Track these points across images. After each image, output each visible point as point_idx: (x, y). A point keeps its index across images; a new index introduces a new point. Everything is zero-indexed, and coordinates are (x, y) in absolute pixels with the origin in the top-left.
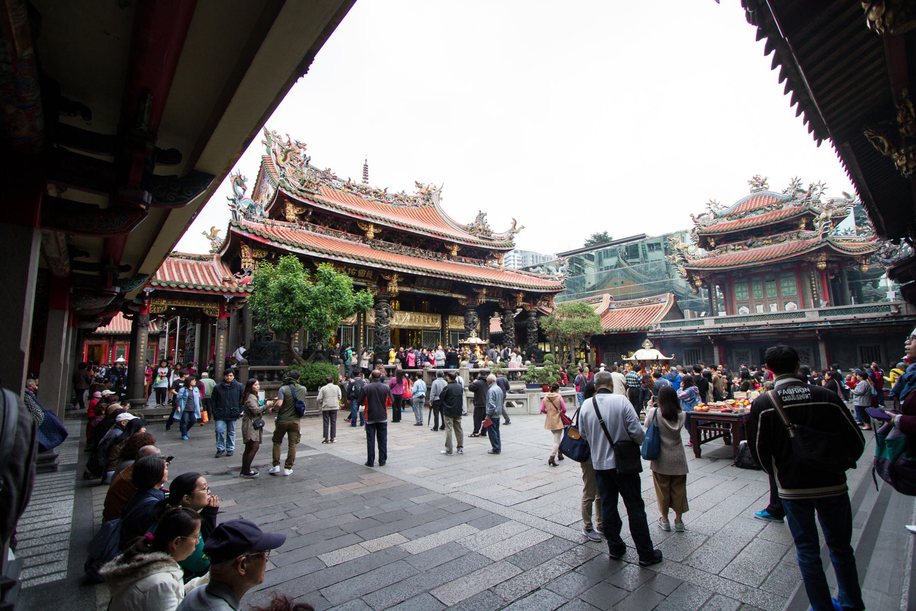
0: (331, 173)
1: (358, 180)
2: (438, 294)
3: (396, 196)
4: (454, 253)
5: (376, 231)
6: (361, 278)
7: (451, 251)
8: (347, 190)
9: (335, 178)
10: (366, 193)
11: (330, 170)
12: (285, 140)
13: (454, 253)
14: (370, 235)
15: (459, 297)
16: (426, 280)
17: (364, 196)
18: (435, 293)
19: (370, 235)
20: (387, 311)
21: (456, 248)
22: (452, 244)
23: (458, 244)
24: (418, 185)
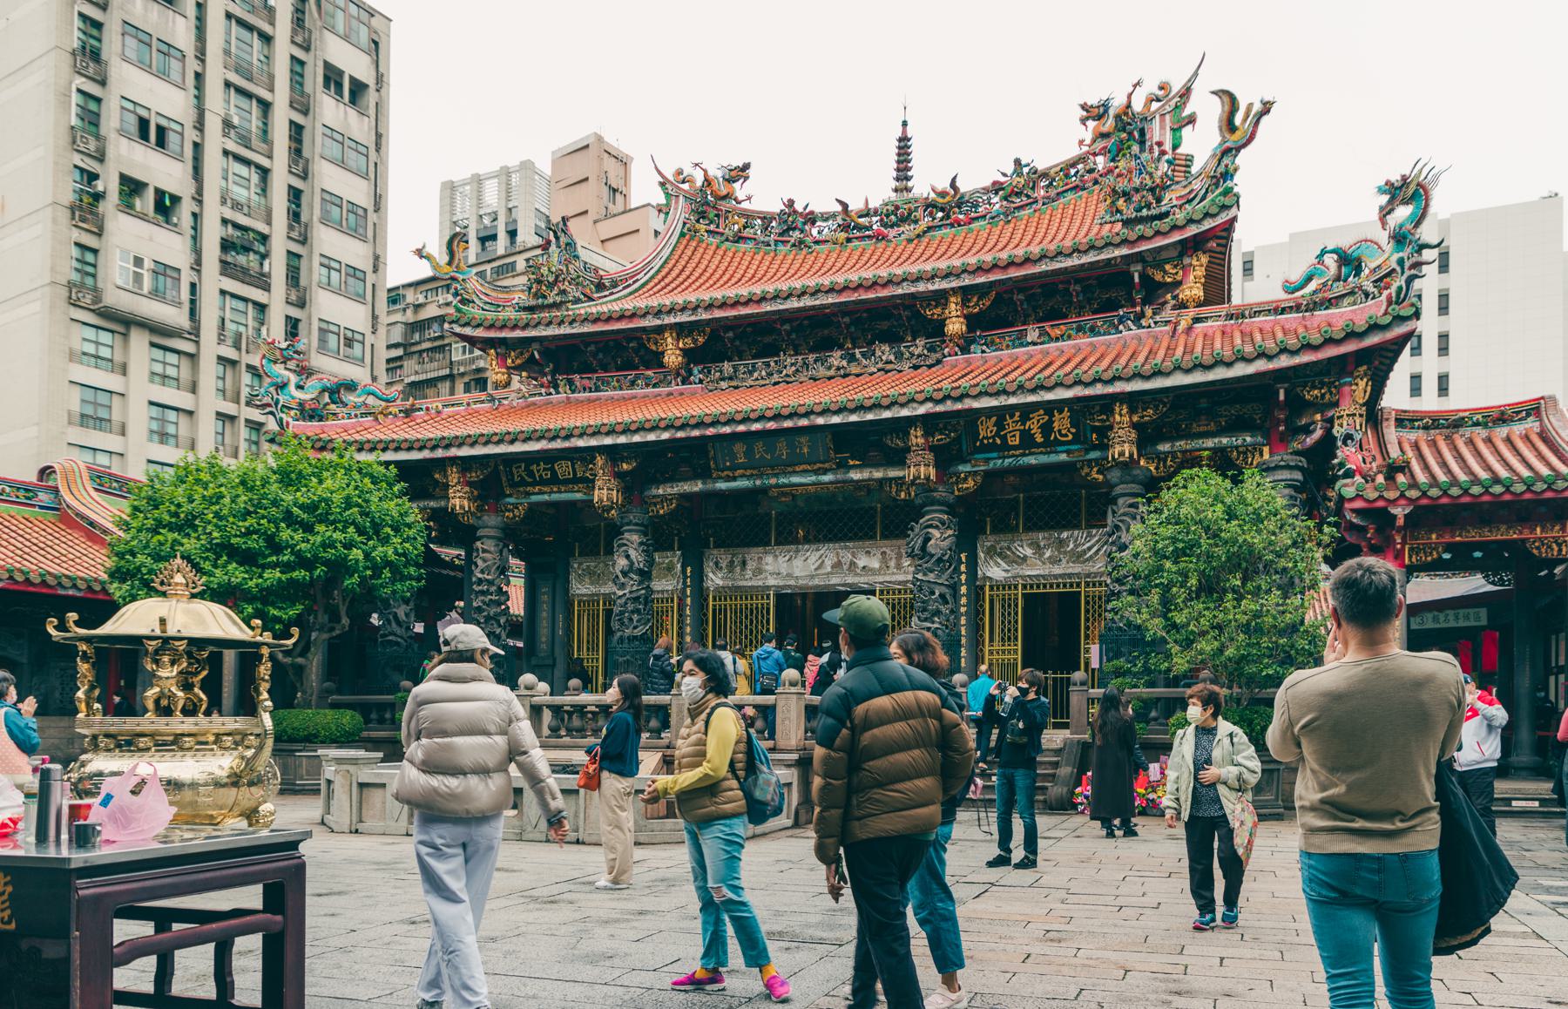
0: (799, 207)
1: (877, 190)
2: (795, 479)
3: (997, 187)
4: (955, 326)
5: (688, 343)
6: (566, 482)
7: (941, 324)
8: (844, 235)
9: (811, 219)
10: (904, 220)
11: (791, 203)
12: (699, 181)
13: (955, 326)
14: (672, 358)
15: (878, 474)
17: (892, 233)
19: (672, 358)
20: (628, 557)
21: (953, 307)
22: (941, 297)
23: (966, 292)
24: (1094, 112)
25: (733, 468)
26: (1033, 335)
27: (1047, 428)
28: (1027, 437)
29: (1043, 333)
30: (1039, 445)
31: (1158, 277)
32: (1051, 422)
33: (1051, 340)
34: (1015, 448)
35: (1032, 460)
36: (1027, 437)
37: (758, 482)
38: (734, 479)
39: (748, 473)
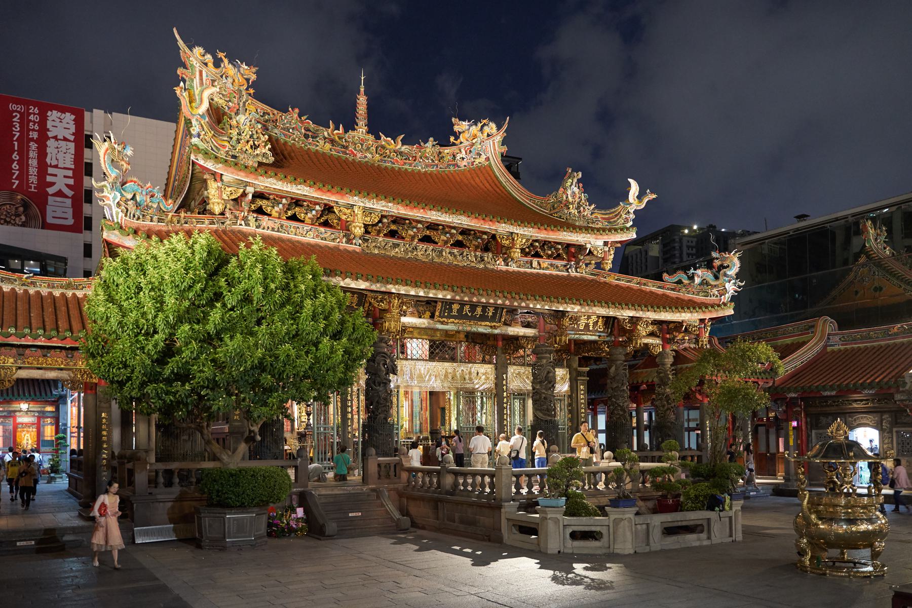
2: (481, 330)
8: (328, 146)
16: (456, 307)
18: (474, 329)
25: (449, 317)
26: (535, 264)
27: (596, 323)
28: (587, 325)
29: (539, 264)
30: (589, 331)
31: (595, 253)
32: (597, 321)
33: (540, 268)
34: (581, 330)
35: (585, 337)
36: (587, 325)
37: (461, 328)
38: (447, 323)
39: (457, 321)
